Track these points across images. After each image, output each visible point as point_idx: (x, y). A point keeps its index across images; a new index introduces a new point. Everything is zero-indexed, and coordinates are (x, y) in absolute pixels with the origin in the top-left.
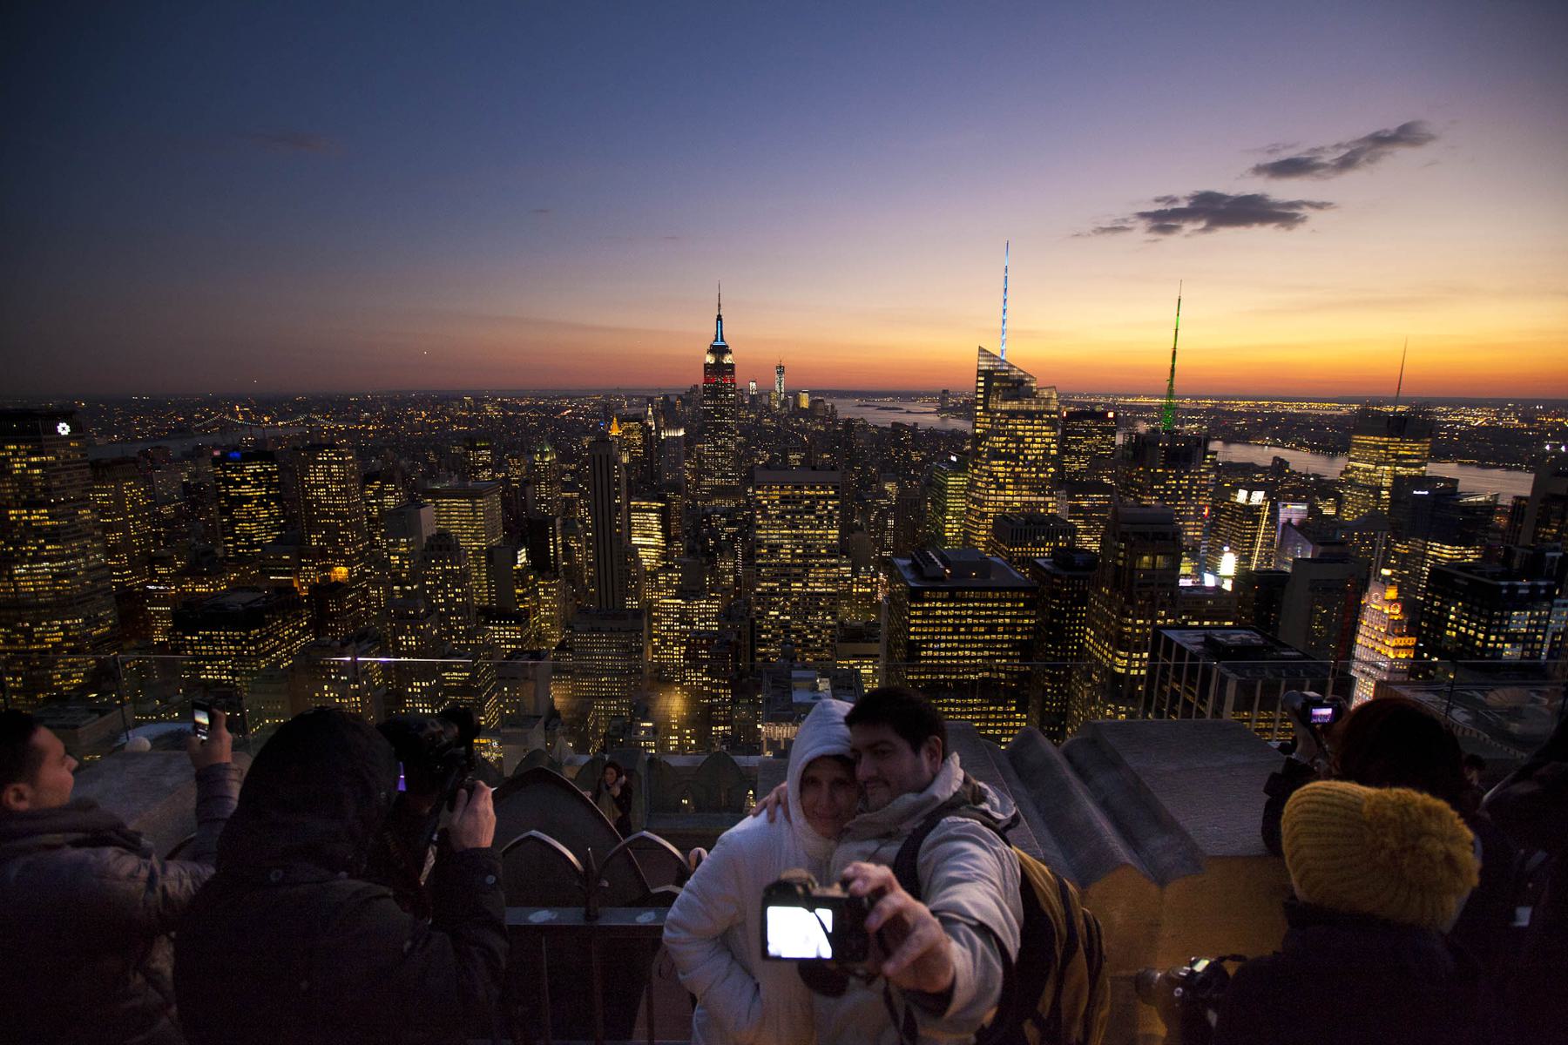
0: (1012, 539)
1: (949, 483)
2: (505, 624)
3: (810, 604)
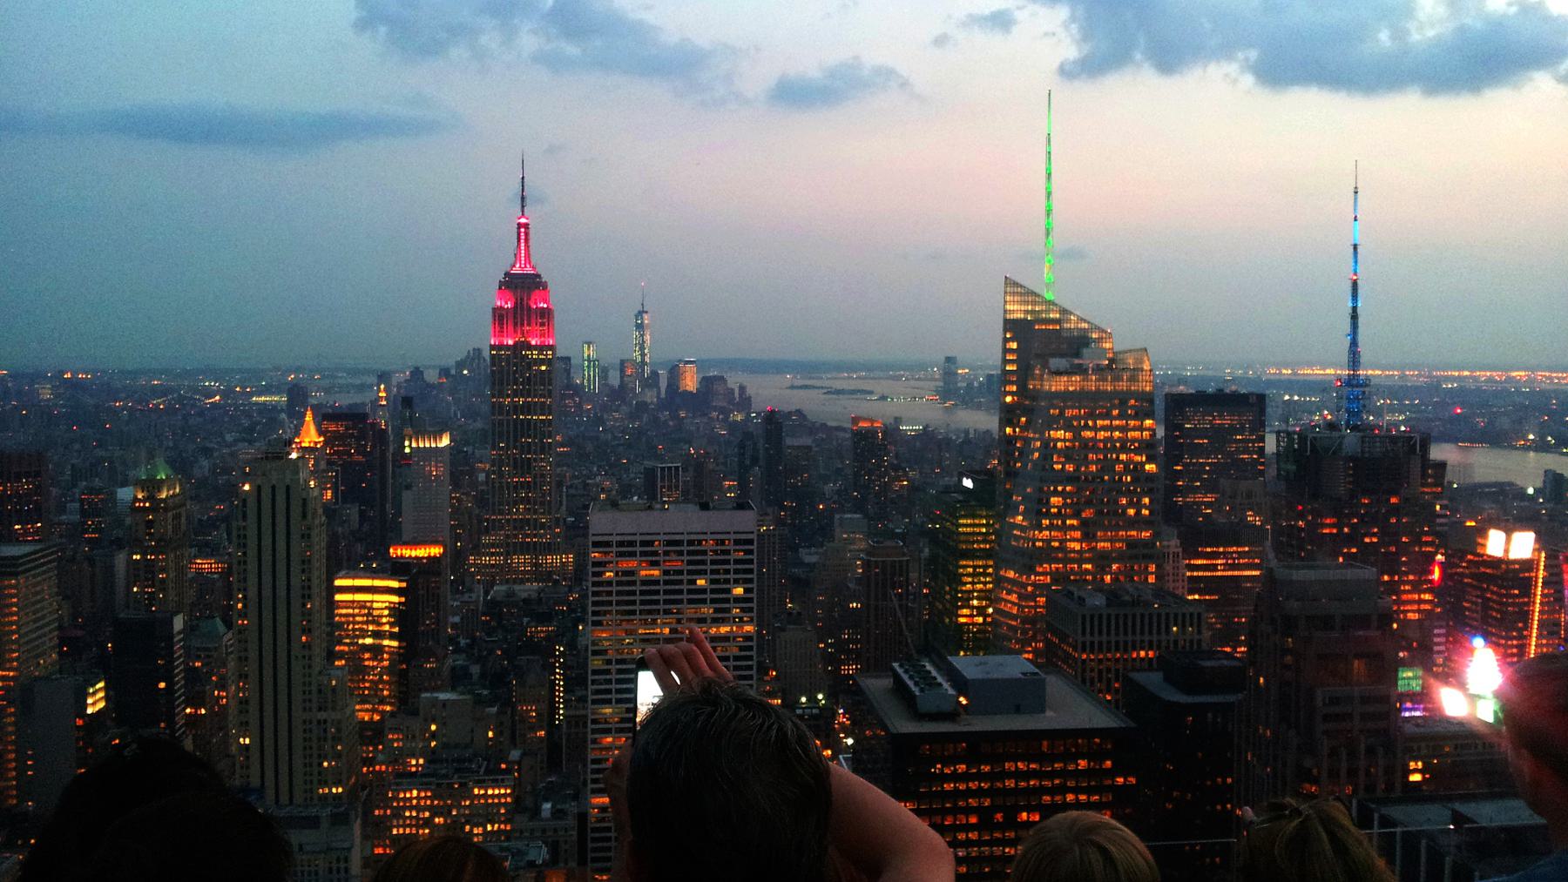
0: (1084, 633)
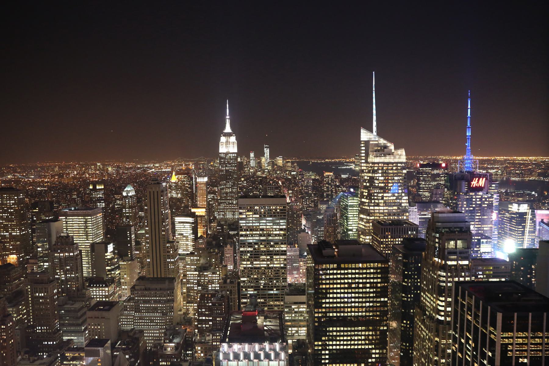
2: (99, 287)
3: (271, 274)
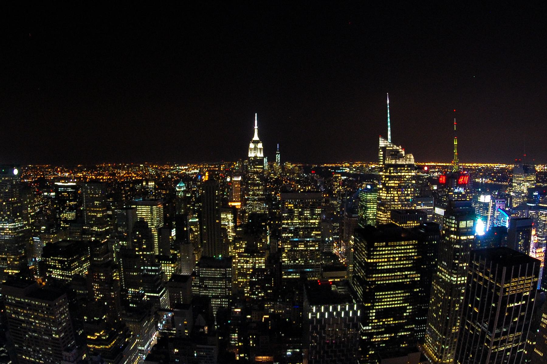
1: (368, 198)
2: (166, 263)
